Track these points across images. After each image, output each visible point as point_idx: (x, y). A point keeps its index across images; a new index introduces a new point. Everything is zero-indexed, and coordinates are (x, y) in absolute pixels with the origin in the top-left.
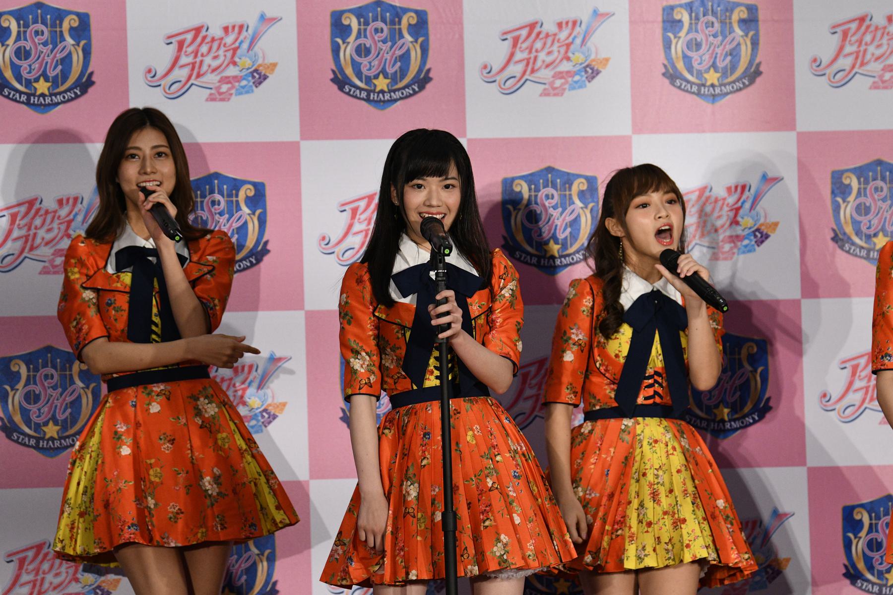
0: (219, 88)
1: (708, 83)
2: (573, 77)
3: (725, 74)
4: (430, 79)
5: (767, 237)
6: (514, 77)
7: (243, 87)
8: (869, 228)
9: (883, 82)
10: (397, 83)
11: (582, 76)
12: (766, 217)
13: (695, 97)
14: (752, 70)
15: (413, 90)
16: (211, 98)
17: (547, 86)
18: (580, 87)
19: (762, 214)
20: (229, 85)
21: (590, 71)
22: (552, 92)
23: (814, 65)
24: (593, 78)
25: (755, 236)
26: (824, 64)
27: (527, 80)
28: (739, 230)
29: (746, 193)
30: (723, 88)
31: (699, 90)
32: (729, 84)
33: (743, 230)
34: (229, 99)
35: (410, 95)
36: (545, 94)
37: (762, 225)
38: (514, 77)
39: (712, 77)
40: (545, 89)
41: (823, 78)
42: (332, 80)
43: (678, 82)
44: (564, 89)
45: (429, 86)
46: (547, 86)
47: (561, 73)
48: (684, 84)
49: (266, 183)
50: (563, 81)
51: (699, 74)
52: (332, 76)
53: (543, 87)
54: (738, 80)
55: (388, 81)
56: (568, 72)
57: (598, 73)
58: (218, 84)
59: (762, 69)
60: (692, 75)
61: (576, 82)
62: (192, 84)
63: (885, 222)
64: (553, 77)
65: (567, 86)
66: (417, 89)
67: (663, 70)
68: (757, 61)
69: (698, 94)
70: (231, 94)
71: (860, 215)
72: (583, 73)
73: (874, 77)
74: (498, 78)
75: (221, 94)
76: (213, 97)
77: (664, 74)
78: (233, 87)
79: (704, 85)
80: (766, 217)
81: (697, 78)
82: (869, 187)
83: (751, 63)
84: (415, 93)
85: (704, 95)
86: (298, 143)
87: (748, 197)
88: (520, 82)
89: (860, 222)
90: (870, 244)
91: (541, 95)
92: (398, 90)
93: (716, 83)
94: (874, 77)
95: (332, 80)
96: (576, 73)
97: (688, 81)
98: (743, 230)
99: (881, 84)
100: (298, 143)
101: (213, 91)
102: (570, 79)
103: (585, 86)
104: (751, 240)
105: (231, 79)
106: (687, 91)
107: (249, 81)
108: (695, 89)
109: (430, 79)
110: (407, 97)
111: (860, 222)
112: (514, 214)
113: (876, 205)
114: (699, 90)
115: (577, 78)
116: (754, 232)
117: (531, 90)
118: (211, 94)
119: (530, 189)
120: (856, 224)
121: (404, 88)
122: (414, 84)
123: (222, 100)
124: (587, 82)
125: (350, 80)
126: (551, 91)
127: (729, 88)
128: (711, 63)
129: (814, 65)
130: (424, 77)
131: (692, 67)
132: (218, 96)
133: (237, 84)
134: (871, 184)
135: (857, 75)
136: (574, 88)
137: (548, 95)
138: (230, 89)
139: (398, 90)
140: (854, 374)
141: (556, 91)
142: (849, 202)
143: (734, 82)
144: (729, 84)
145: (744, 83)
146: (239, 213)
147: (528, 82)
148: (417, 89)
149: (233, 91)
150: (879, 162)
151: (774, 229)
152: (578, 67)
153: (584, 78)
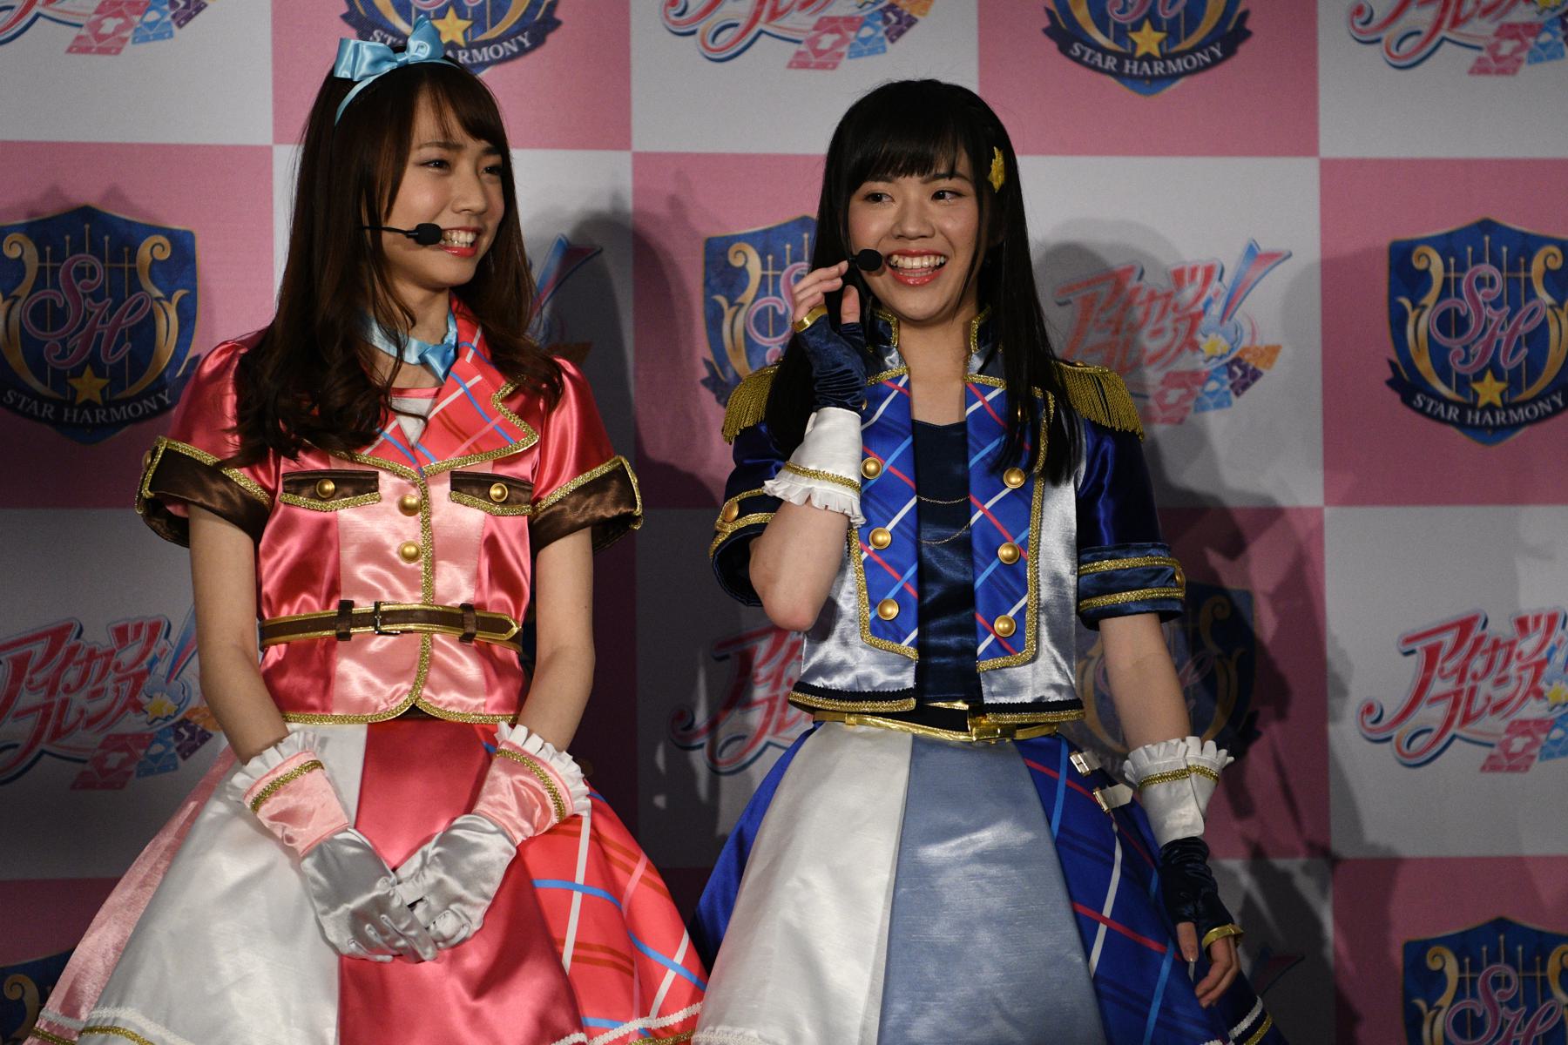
0: (98, 24)
1: (1140, 52)
2: (858, 29)
3: (1173, 34)
4: (558, 23)
5: (1256, 375)
6: (735, 25)
7: (151, 25)
8: (1466, 361)
9: (1498, 59)
10: (485, 30)
11: (877, 29)
12: (1253, 333)
13: (1112, 80)
14: (1230, 27)
15: (520, 44)
16: (79, 47)
17: (802, 48)
18: (873, 52)
19: (1247, 328)
20: (120, 21)
21: (894, 19)
22: (813, 60)
23: (1358, 21)
24: (900, 33)
25: (1232, 374)
26: (1379, 16)
27: (761, 32)
28: (1198, 362)
29: (1215, 285)
30: (1170, 63)
31: (1120, 65)
32: (1181, 54)
33: (1206, 361)
34: (118, 51)
35: (513, 57)
36: (799, 63)
37: (1245, 350)
38: (735, 25)
39: (1148, 40)
40: (799, 54)
41: (1376, 47)
42: (345, 17)
43: (1077, 49)
44: (840, 55)
45: (552, 38)
46: (802, 48)
47: (833, 20)
48: (1089, 51)
49: (196, 232)
50: (837, 37)
51: (1121, 34)
52: (345, 9)
53: (794, 48)
54: (1199, 48)
55: (465, 24)
56: (849, 20)
57: (911, 22)
58: (95, 17)
59: (1249, 25)
60: (1106, 35)
61: (865, 41)
62: (38, 15)
63: (1498, 348)
64: (816, 28)
65: (845, 49)
66: (527, 45)
67: (1046, 23)
68: (1240, 9)
69: (1118, 74)
70: (124, 40)
71: (1446, 333)
72: (879, 23)
73: (1479, 48)
74: (700, 27)
75: (101, 38)
76: (83, 44)
77: (1046, 31)
78: (128, 25)
79: (1131, 57)
80: (1253, 333)
81: (1115, 41)
82: (1466, 277)
83: (1225, 17)
84: (523, 51)
85: (1131, 76)
86: (270, 149)
87: (1216, 295)
88: (745, 38)
89: (1448, 350)
90: (1467, 396)
91: (790, 66)
92: (488, 43)
93: (1156, 52)
94: (1479, 48)
95: (345, 17)
96: (863, 23)
97: (1098, 48)
98: (1206, 361)
99: (1493, 64)
100: (270, 149)
101: (84, 32)
102: (852, 34)
103: (884, 50)
104: (1222, 383)
105: (123, 8)
106: (1095, 68)
107: (163, 13)
108: (1111, 63)
109: (558, 23)
110: (505, 59)
111: (1448, 350)
112: (728, 313)
113: (1479, 312)
114: (1120, 65)
115: (866, 32)
116: (1229, 365)
117: (769, 54)
118: (79, 38)
119: (764, 266)
120: (1439, 356)
121: (499, 40)
122: (520, 32)
123: (103, 51)
124: (887, 43)
125: (385, 19)
126: (812, 59)
127: (1181, 64)
128: (1144, 11)
129: (1358, 21)
130: (542, 21)
131: (1108, 18)
132: (95, 45)
133: (137, 18)
134: (1471, 270)
135: (1446, 45)
136: (859, 54)
137: (805, 65)
138: (119, 29)
139: (488, 43)
140: (1430, 664)
141: (821, 60)
142: (1424, 307)
143: (1192, 51)
144: (1181, 54)
145: (1212, 55)
146: (136, 296)
147: (763, 36)
148: (527, 45)
149: (128, 34)
150: (1487, 226)
151: (1271, 361)
152: (868, 10)
153: (881, 34)
